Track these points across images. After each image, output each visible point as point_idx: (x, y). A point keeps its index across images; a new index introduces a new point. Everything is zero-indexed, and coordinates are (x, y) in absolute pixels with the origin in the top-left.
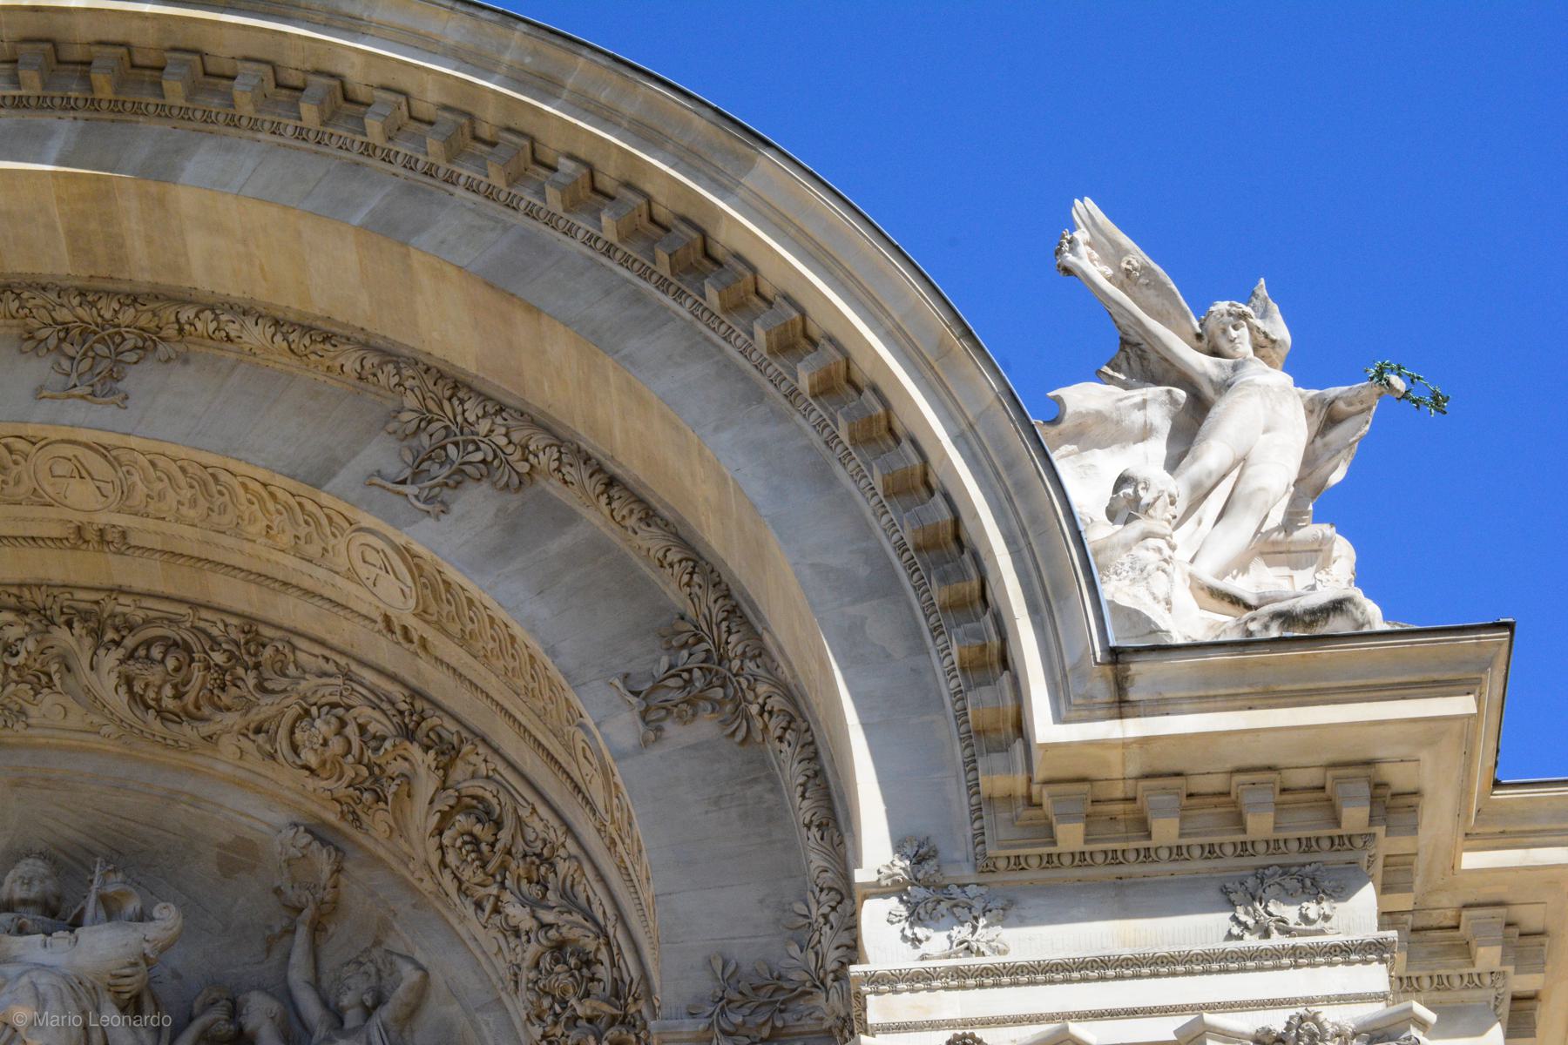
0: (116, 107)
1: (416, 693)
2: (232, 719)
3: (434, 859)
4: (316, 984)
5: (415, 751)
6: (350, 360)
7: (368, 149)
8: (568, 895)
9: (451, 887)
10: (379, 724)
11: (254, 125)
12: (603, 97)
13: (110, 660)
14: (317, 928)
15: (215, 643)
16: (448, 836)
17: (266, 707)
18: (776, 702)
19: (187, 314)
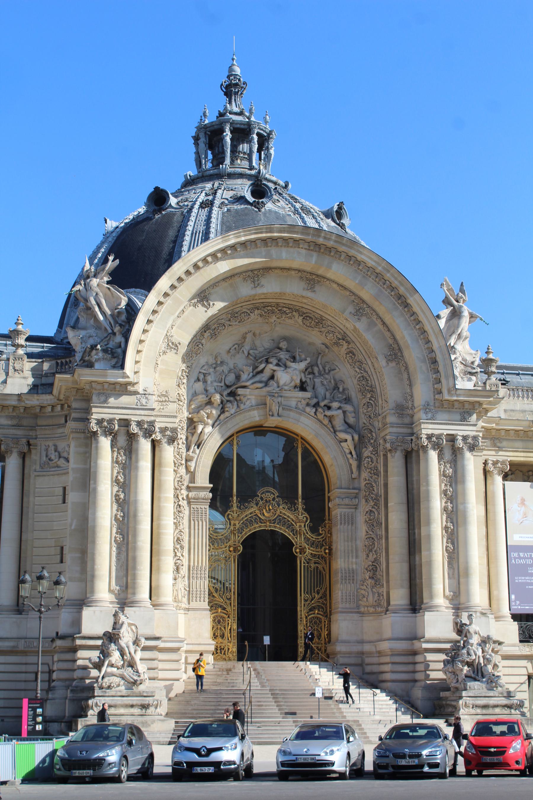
0: (323, 253)
1: (345, 333)
2: (317, 329)
3: (345, 357)
5: (344, 342)
6: (348, 293)
7: (358, 269)
8: (364, 369)
9: (347, 361)
10: (339, 336)
11: (342, 260)
12: (396, 276)
13: (301, 318)
15: (316, 319)
16: (348, 356)
17: (323, 329)
18: (404, 365)
19: (325, 280)
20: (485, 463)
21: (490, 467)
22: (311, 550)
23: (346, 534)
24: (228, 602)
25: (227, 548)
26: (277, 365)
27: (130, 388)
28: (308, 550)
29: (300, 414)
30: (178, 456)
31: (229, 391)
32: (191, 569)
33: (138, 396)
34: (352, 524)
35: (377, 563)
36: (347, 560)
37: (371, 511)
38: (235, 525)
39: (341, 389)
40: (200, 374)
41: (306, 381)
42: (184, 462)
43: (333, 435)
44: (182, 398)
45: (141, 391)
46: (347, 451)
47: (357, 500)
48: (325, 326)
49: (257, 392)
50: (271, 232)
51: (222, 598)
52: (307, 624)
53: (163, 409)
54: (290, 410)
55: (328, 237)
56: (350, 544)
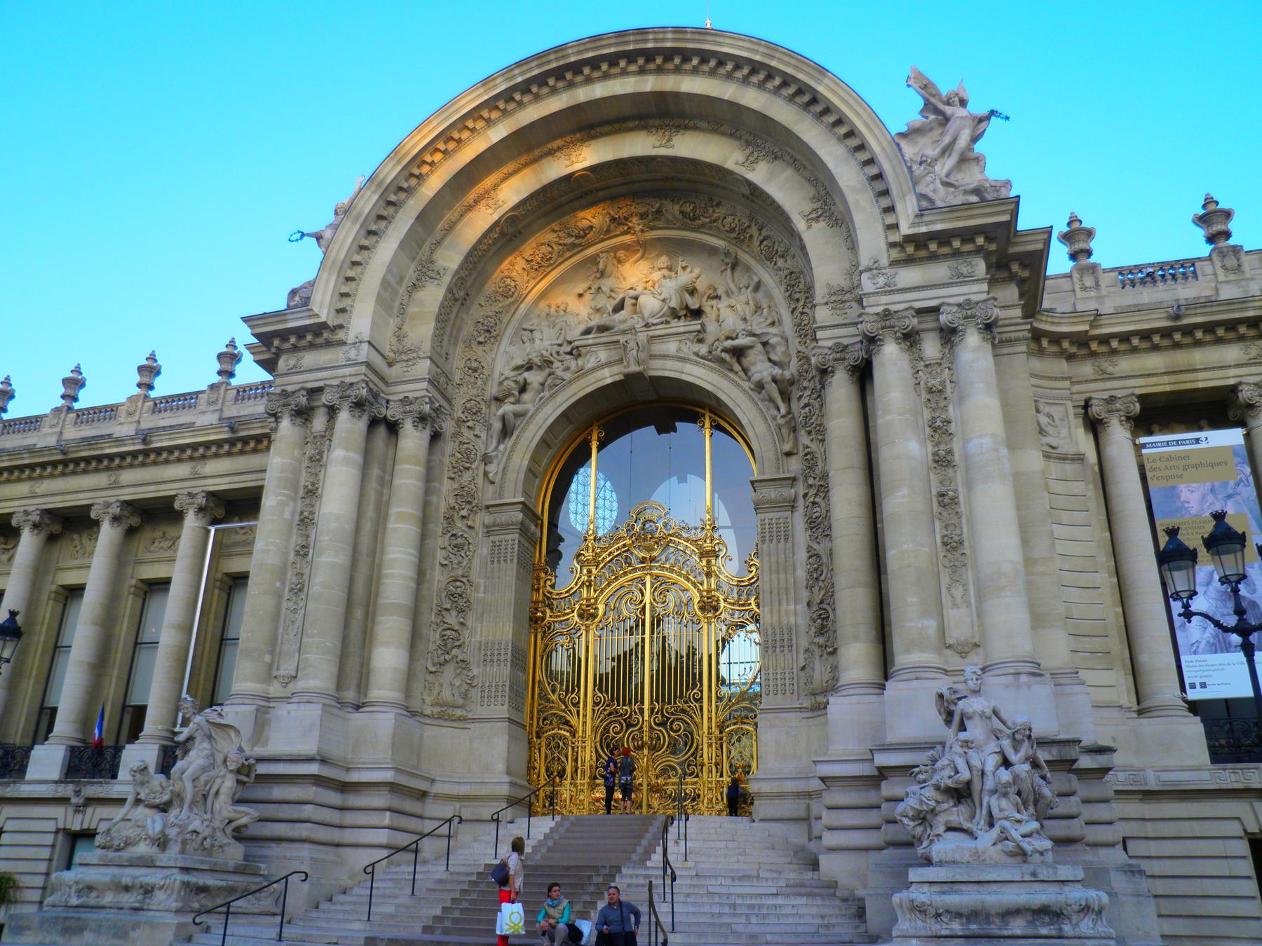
4: (733, 281)
13: (677, 207)
14: (733, 268)
19: (687, 122)
20: (1087, 405)
21: (1097, 409)
22: (730, 604)
23: (773, 559)
24: (574, 710)
25: (575, 614)
28: (722, 604)
29: (684, 360)
30: (459, 456)
31: (568, 349)
32: (483, 647)
33: (347, 348)
34: (786, 540)
35: (828, 604)
36: (776, 607)
37: (814, 503)
38: (589, 572)
39: (765, 311)
40: (524, 333)
43: (746, 385)
44: (475, 365)
45: (351, 339)
46: (771, 405)
47: (793, 491)
48: (718, 210)
49: (605, 337)
50: (563, 57)
51: (564, 703)
52: (721, 746)
53: (407, 371)
54: (665, 357)
55: (661, 36)
56: (782, 576)
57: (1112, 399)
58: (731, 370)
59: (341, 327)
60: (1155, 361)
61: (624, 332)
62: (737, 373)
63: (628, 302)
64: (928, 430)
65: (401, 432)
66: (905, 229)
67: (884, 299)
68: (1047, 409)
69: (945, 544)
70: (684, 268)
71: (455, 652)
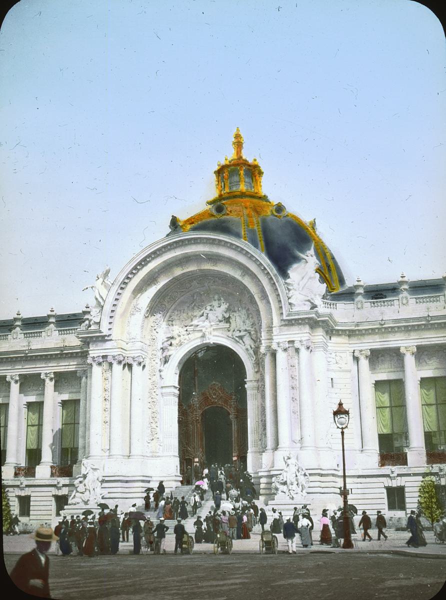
26: (211, 310)
27: (106, 338)
41: (229, 317)
42: (158, 374)
44: (154, 337)
57: (361, 351)
58: (239, 342)
59: (110, 335)
60: (377, 338)
61: (204, 327)
62: (240, 343)
63: (205, 315)
64: (291, 378)
65: (133, 367)
66: (285, 318)
67: (279, 337)
68: (341, 354)
69: (293, 412)
70: (223, 303)
71: (155, 435)
